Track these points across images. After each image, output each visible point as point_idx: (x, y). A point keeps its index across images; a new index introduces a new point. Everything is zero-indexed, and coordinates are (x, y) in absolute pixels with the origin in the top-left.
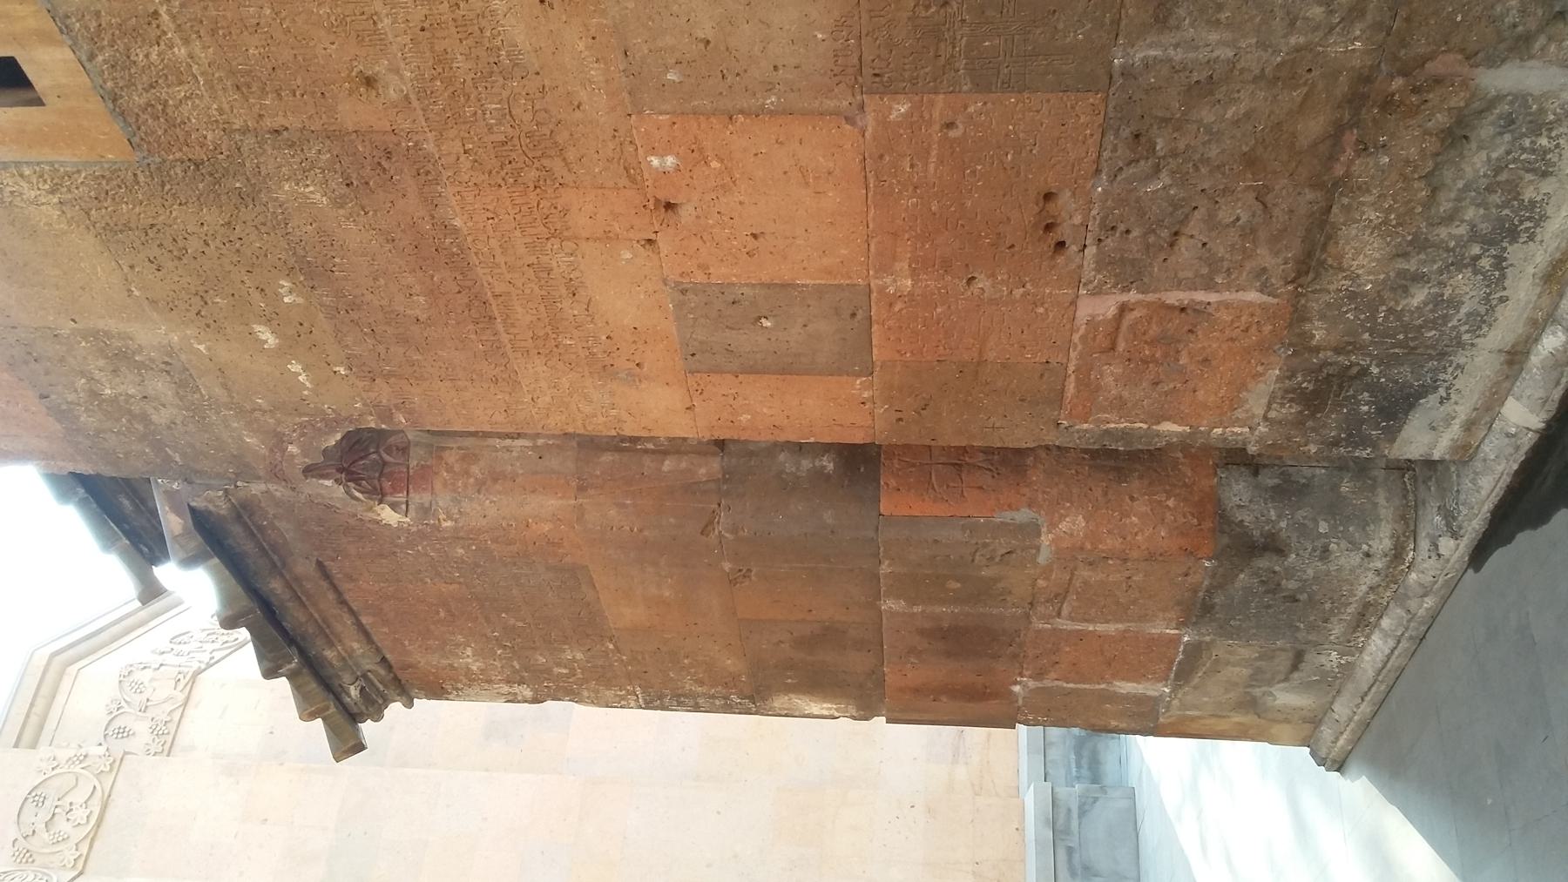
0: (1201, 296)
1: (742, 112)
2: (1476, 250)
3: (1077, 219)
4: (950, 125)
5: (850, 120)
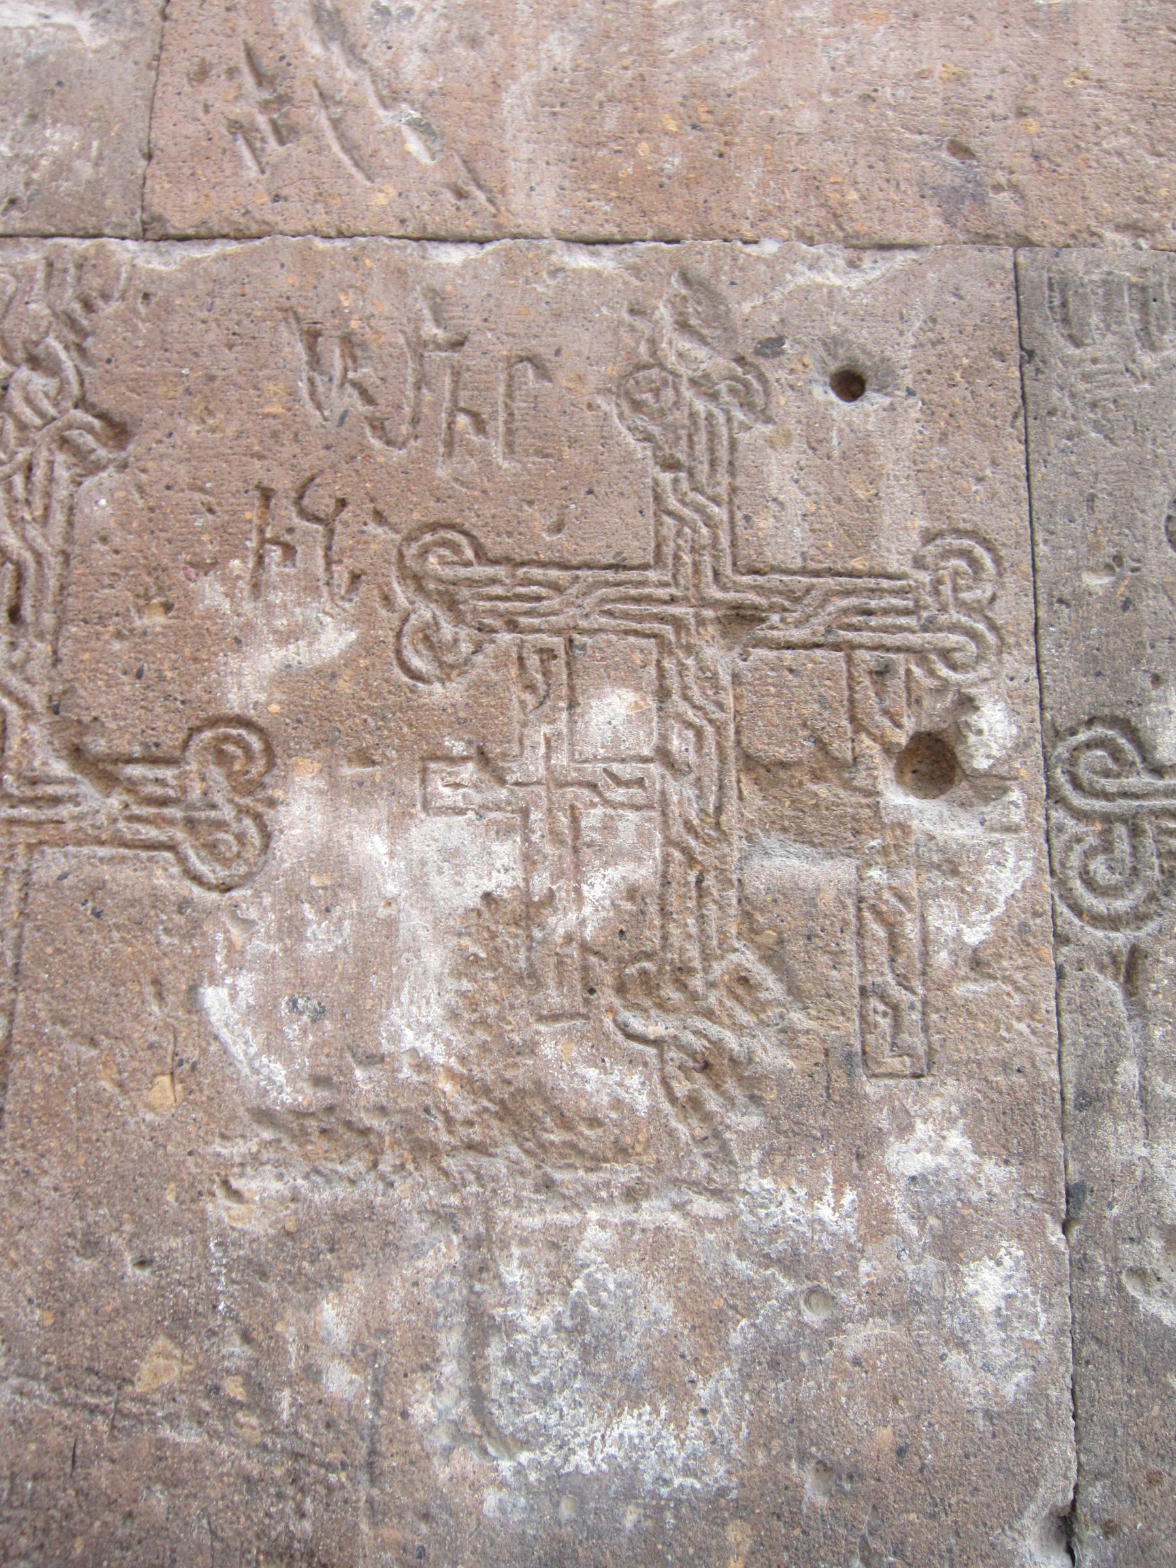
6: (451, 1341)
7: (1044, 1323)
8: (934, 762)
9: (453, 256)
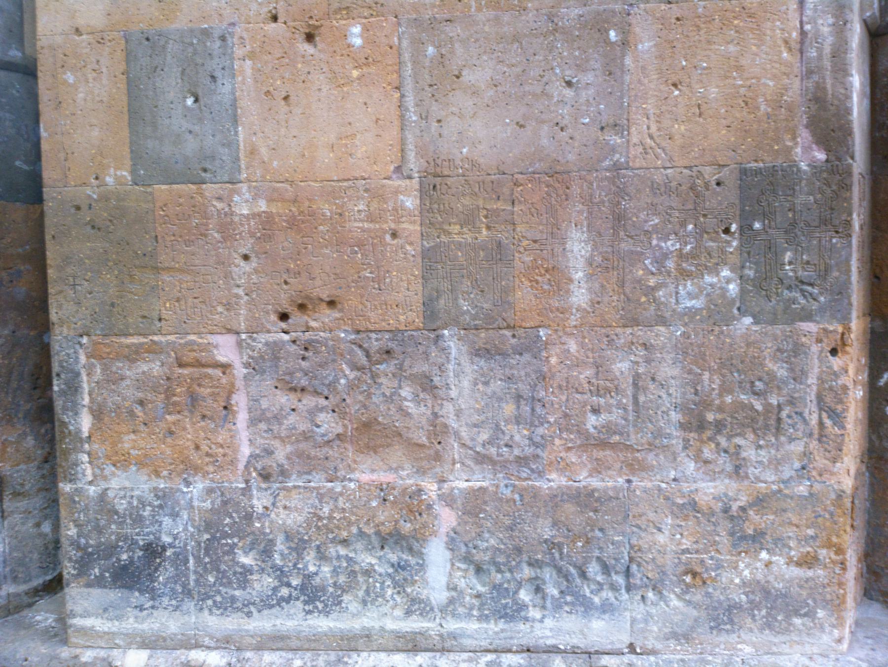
0: (242, 417)
1: (402, 96)
2: (294, 583)
3: (313, 324)
4: (394, 235)
5: (398, 169)
6: (674, 295)
7: (737, 289)
8: (727, 231)
9: (669, 171)
